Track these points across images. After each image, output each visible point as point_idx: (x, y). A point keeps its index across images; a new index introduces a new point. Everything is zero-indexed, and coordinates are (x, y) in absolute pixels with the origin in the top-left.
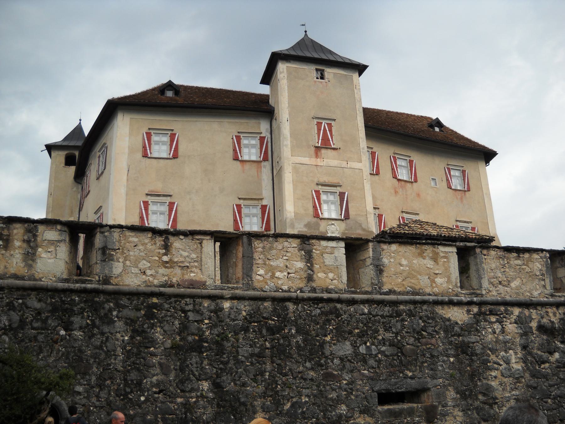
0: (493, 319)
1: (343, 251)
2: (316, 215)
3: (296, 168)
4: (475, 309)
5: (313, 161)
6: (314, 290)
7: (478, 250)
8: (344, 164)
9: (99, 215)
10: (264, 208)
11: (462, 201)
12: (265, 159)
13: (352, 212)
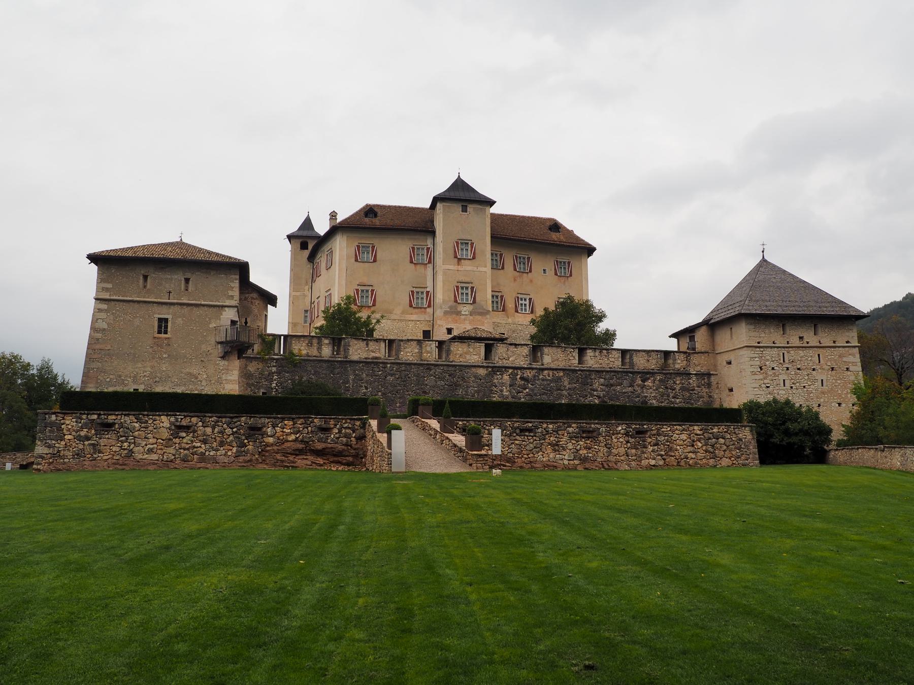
2: (456, 301)
3: (445, 272)
4: (490, 370)
6: (422, 360)
9: (329, 293)
10: (428, 292)
13: (478, 299)
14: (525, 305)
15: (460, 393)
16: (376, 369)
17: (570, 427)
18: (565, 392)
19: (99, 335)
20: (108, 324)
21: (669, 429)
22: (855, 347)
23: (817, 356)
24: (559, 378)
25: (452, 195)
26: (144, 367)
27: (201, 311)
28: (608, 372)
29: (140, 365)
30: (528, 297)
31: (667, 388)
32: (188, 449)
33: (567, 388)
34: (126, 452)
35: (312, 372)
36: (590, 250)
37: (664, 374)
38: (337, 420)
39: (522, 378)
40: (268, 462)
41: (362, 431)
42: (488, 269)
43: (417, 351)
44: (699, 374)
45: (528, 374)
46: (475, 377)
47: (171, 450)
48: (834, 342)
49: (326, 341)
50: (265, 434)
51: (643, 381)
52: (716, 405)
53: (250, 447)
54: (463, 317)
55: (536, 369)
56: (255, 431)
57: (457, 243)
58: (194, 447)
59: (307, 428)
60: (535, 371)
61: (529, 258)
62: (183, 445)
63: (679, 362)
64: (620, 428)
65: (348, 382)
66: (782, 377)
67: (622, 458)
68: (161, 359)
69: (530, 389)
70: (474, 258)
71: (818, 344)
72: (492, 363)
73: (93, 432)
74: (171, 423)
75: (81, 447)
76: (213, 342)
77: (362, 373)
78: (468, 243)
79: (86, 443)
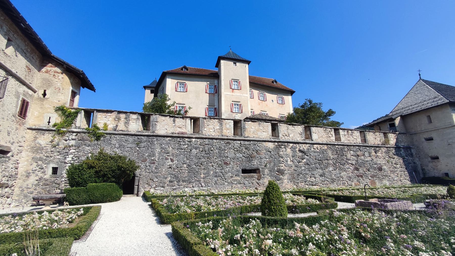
1: (233, 123)
4: (276, 144)
5: (231, 94)
6: (223, 136)
7: (279, 124)
8: (242, 95)
10: (215, 109)
12: (216, 93)
15: (255, 164)
16: (181, 143)
18: (331, 162)
24: (326, 150)
28: (354, 146)
33: (331, 158)
37: (387, 147)
39: (300, 151)
43: (218, 127)
44: (405, 148)
45: (304, 147)
60: (308, 145)
65: (154, 155)
77: (169, 147)
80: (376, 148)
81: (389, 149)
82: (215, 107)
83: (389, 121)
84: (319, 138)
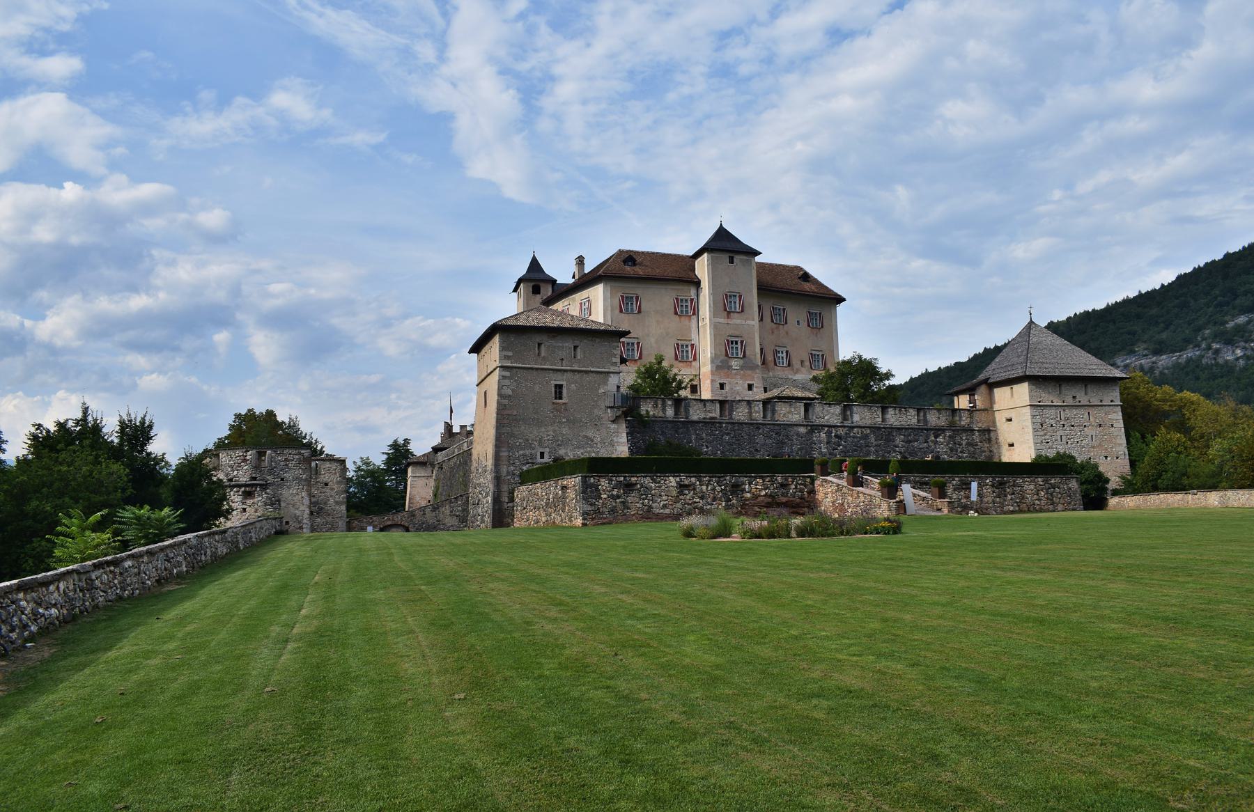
0: (816, 432)
2: (727, 355)
4: (809, 428)
6: (751, 420)
8: (744, 322)
10: (693, 345)
11: (816, 336)
14: (782, 357)
17: (954, 480)
18: (872, 449)
19: (506, 401)
20: (513, 391)
21: (1021, 481)
22: (1117, 405)
23: (1087, 414)
25: (719, 245)
26: (548, 431)
27: (590, 377)
28: (906, 429)
29: (543, 430)
30: (785, 350)
31: (955, 443)
32: (690, 504)
34: (646, 508)
35: (660, 432)
36: (840, 300)
37: (953, 430)
38: (794, 478)
40: (749, 513)
41: (811, 486)
42: (755, 323)
43: (747, 411)
45: (841, 432)
46: (797, 435)
47: (679, 505)
48: (1101, 401)
49: (670, 403)
50: (744, 490)
51: (936, 437)
52: (996, 460)
53: (734, 501)
54: (734, 372)
55: (848, 426)
56: (736, 488)
57: (726, 295)
58: (695, 502)
59: (773, 485)
60: (847, 429)
61: (784, 309)
62: (687, 501)
63: (964, 419)
64: (988, 481)
65: (691, 442)
66: (1059, 433)
67: (990, 505)
68: (561, 423)
69: (845, 447)
70: (742, 311)
71: (1088, 403)
72: (811, 422)
73: (622, 491)
74: (677, 483)
75: (614, 504)
76: (603, 407)
78: (735, 296)
79: (618, 501)
80: (938, 431)
81: (956, 432)
82: (693, 343)
83: (970, 391)
84: (861, 420)
